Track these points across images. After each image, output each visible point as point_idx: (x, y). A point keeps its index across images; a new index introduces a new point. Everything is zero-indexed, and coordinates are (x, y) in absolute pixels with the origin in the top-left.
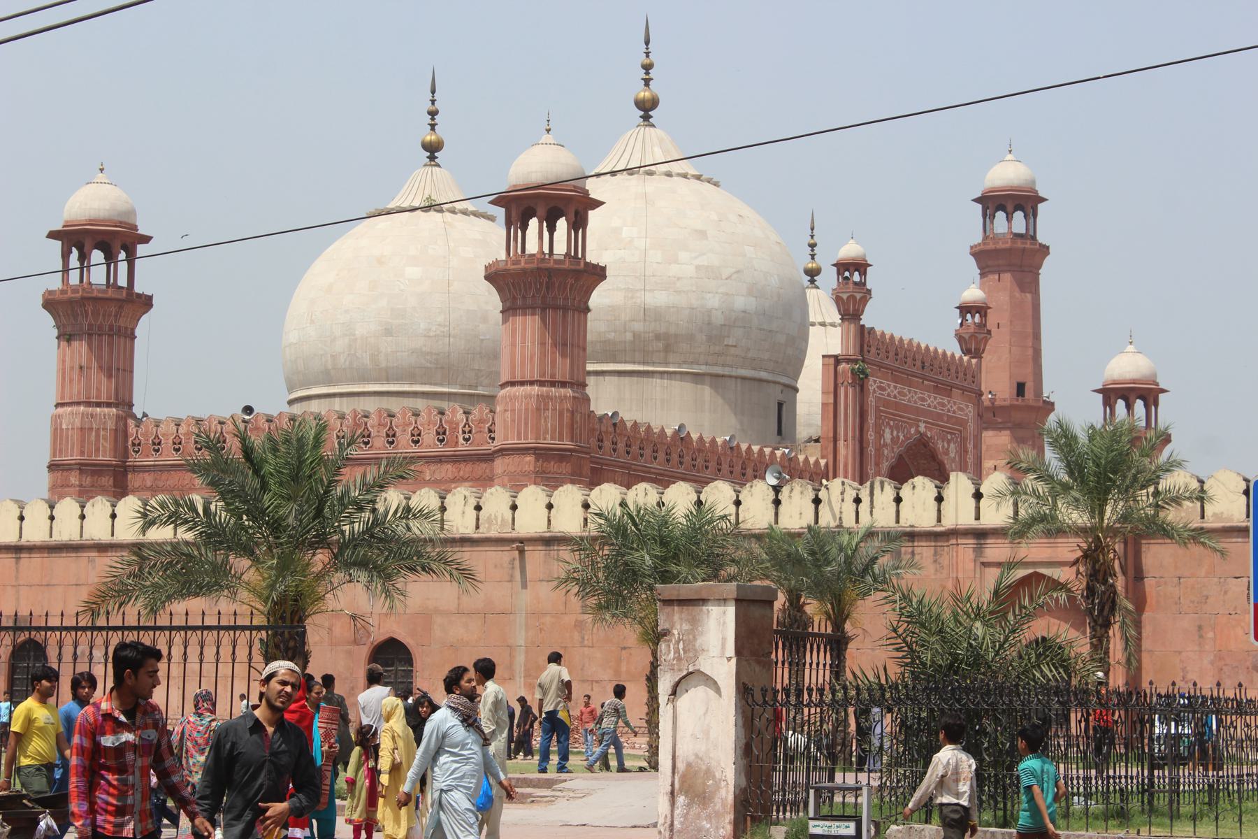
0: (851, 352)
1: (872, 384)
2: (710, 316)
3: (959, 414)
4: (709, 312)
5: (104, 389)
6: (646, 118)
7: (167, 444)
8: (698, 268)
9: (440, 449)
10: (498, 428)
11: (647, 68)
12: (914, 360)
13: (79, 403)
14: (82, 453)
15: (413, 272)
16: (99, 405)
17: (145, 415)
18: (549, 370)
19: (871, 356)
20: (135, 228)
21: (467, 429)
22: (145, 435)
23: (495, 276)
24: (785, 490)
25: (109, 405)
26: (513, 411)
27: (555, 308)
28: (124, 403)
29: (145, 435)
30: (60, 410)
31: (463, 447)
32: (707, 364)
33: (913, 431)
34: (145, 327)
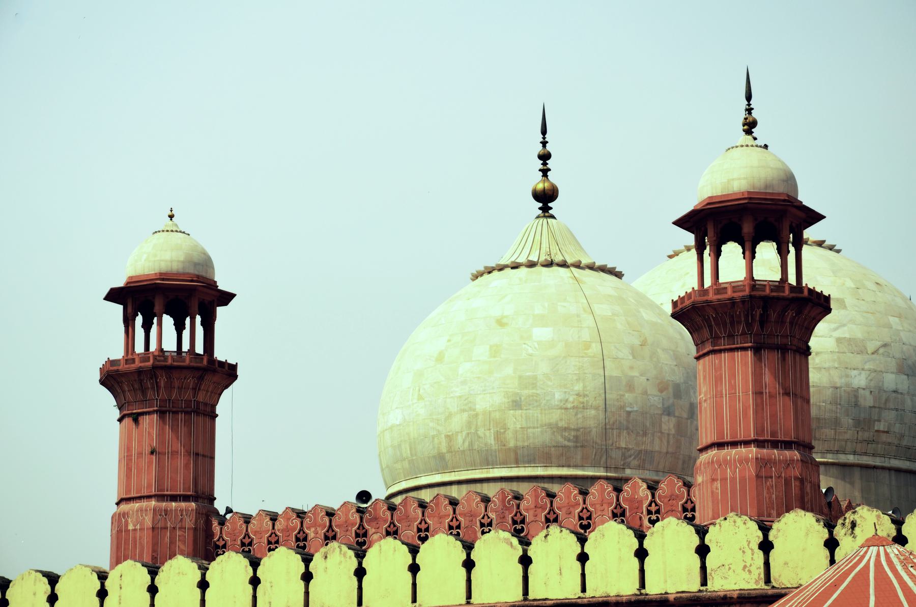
2: (856, 397)
4: (855, 393)
5: (180, 478)
8: (839, 341)
13: (149, 497)
15: (543, 334)
16: (174, 498)
17: (229, 510)
21: (653, 508)
22: (233, 534)
25: (186, 498)
26: (724, 480)
28: (203, 495)
30: (125, 507)
32: (855, 453)
34: (229, 404)
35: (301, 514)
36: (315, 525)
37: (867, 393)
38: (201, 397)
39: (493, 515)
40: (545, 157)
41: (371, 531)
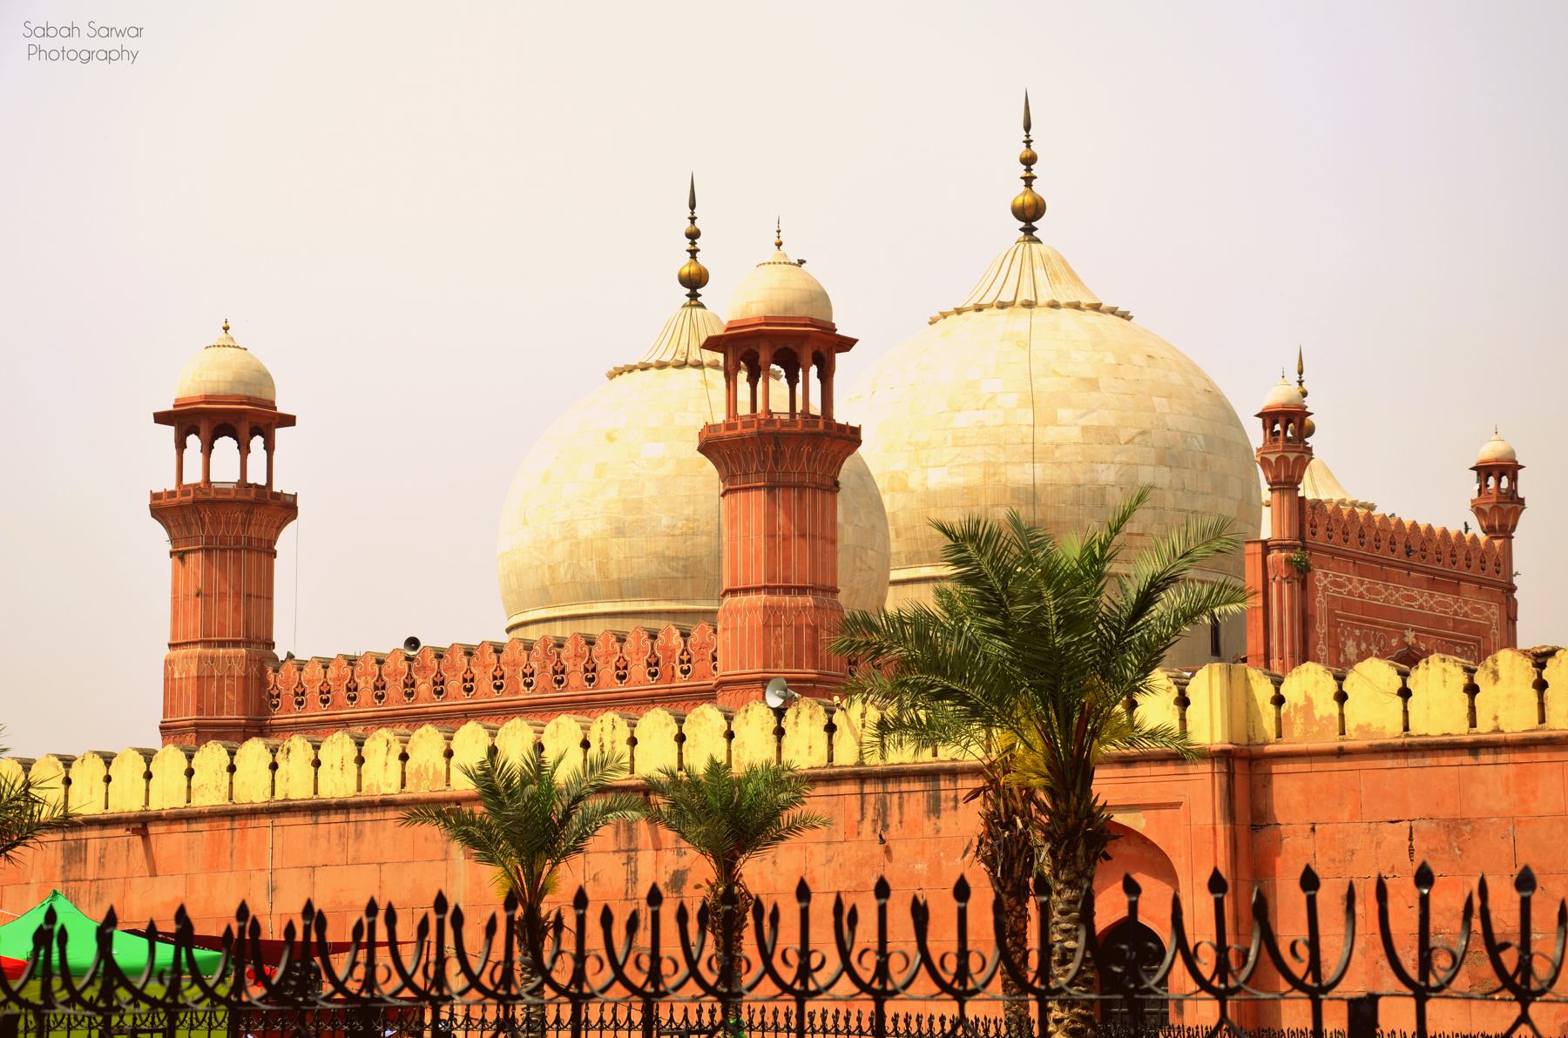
0: (1286, 535)
1: (1321, 578)
2: (1103, 496)
3: (1474, 618)
4: (1102, 490)
5: (229, 622)
6: (1029, 231)
7: (313, 693)
8: (1085, 429)
9: (652, 685)
10: (719, 655)
11: (1029, 161)
12: (1393, 543)
13: (195, 643)
14: (199, 711)
16: (222, 644)
17: (290, 656)
18: (780, 571)
19: (1320, 538)
20: (272, 405)
21: (685, 658)
22: (286, 682)
23: (711, 446)
24: (790, 714)
25: (236, 644)
27: (788, 486)
29: (286, 682)
31: (681, 681)
33: (1394, 642)
34: (286, 541)
35: (352, 661)
36: (365, 674)
37: (1117, 490)
38: (253, 532)
39: (535, 665)
40: (693, 235)
41: (419, 681)
